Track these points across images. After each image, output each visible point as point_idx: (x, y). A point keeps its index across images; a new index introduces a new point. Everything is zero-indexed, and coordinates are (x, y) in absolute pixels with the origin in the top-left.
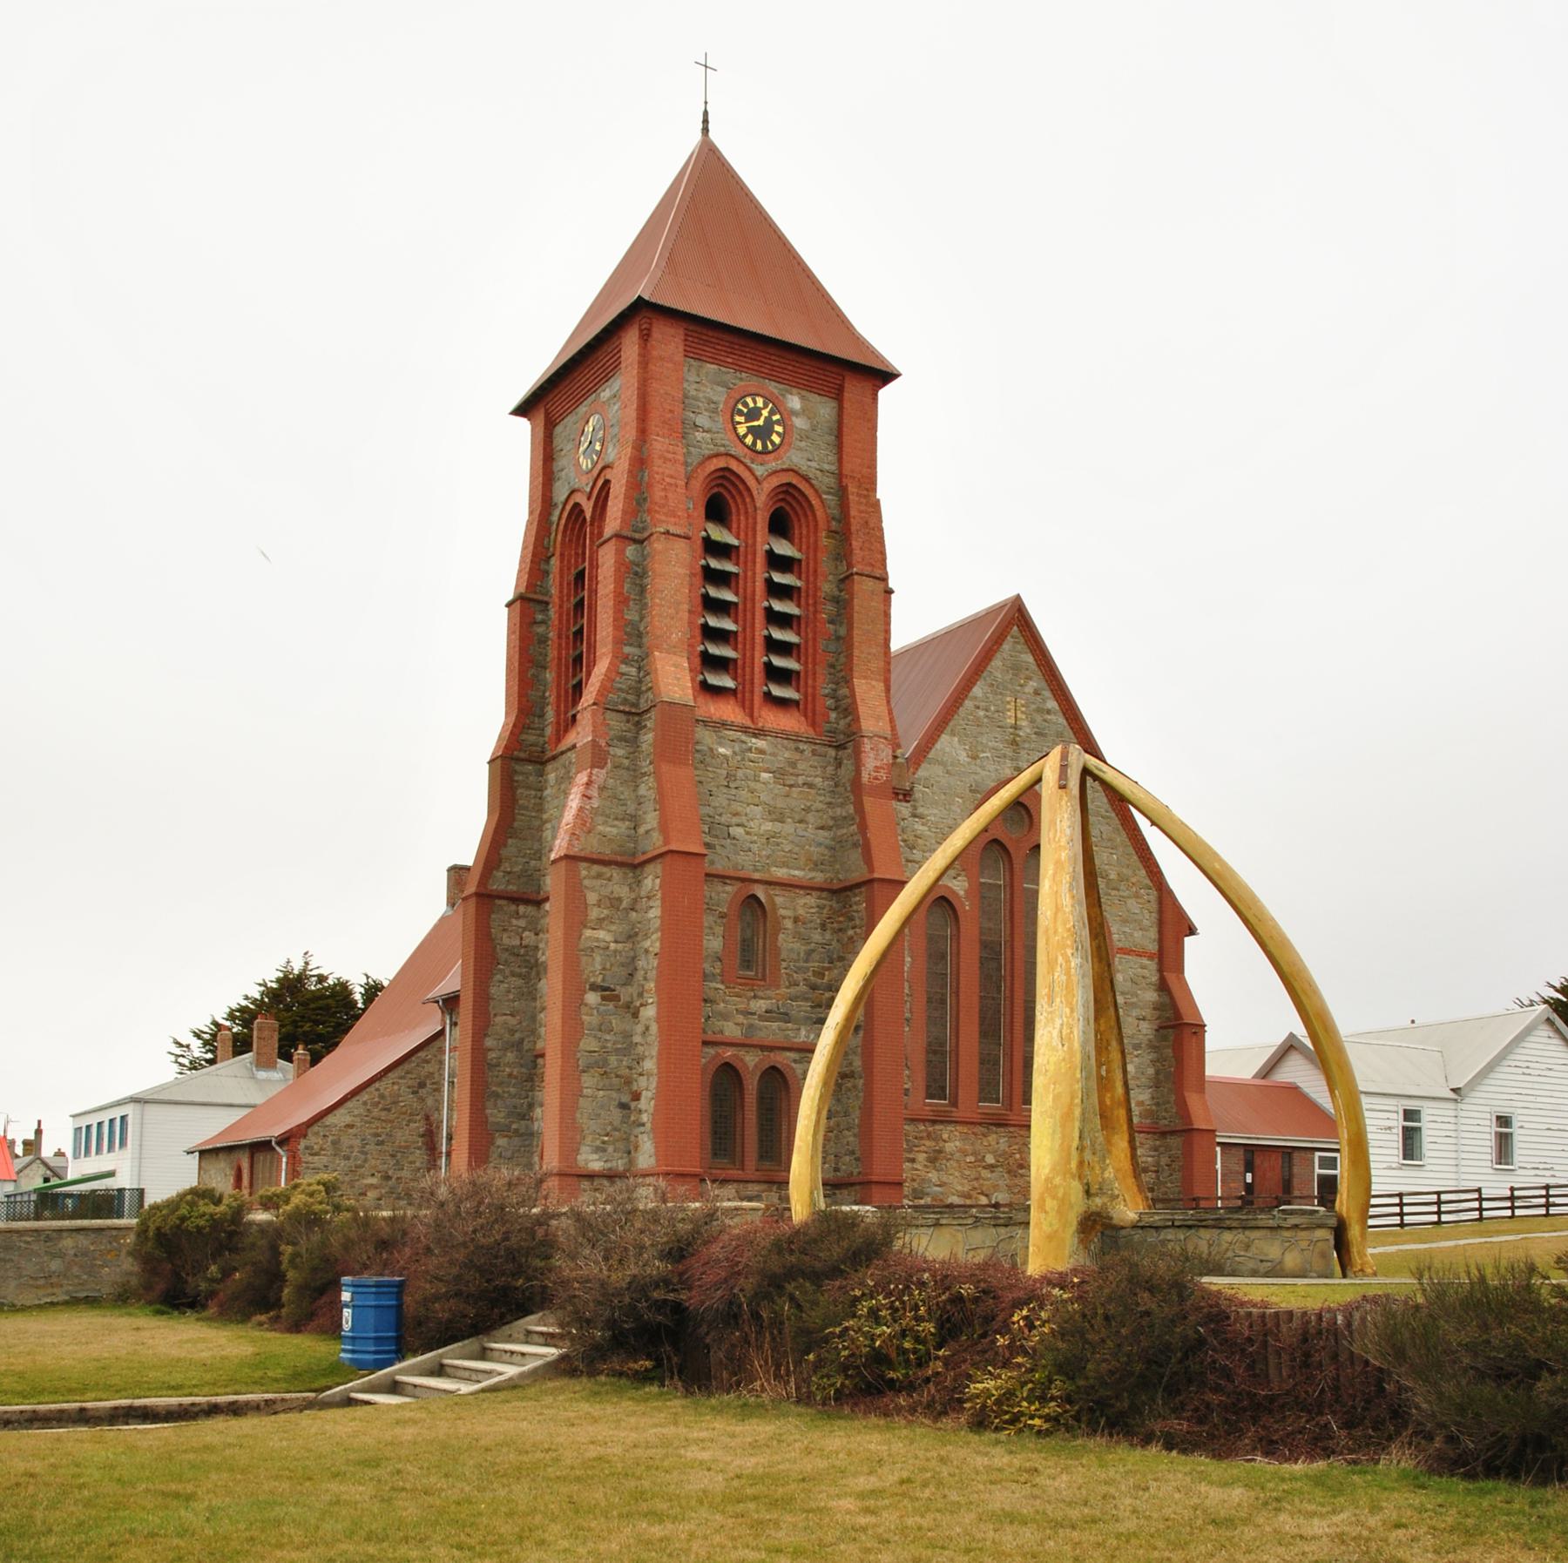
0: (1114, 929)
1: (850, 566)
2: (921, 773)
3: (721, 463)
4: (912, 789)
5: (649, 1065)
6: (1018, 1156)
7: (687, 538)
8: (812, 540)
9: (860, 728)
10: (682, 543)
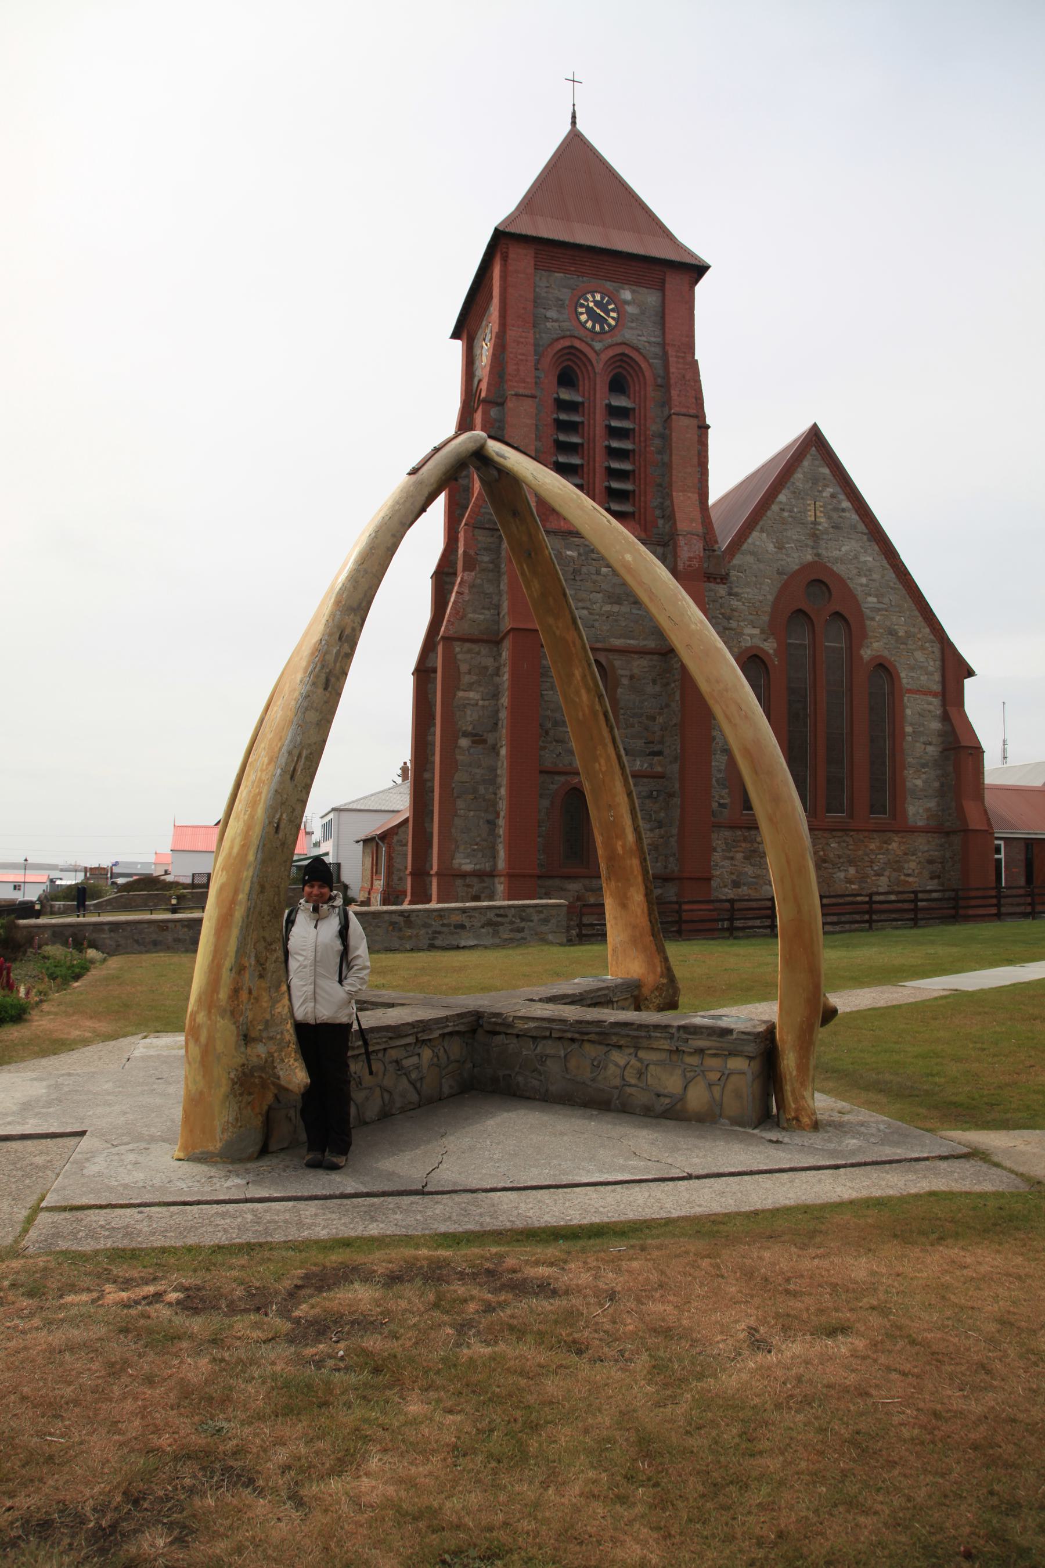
0: (903, 675)
1: (670, 409)
2: (735, 562)
3: (567, 343)
4: (728, 574)
5: (503, 791)
6: (821, 853)
7: (534, 397)
8: (642, 393)
9: (676, 530)
10: (530, 401)
